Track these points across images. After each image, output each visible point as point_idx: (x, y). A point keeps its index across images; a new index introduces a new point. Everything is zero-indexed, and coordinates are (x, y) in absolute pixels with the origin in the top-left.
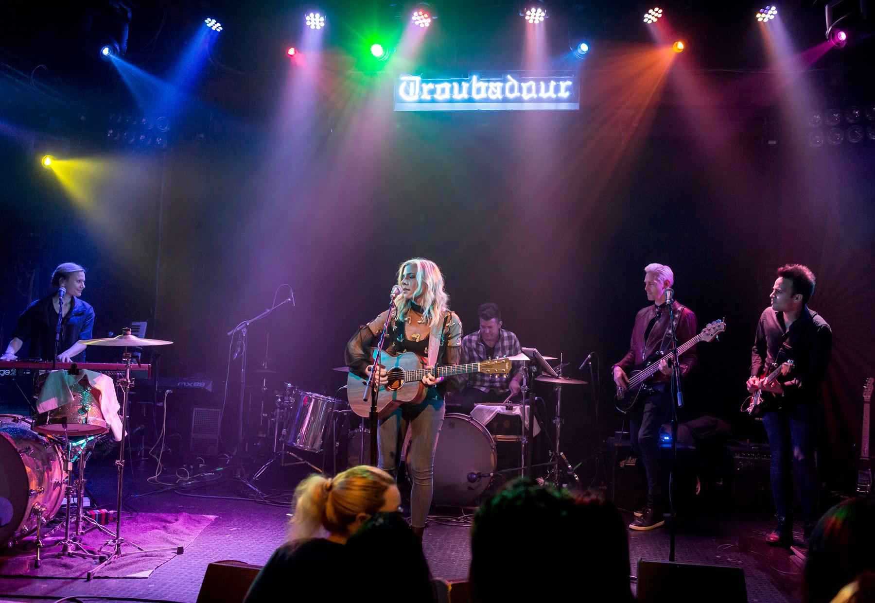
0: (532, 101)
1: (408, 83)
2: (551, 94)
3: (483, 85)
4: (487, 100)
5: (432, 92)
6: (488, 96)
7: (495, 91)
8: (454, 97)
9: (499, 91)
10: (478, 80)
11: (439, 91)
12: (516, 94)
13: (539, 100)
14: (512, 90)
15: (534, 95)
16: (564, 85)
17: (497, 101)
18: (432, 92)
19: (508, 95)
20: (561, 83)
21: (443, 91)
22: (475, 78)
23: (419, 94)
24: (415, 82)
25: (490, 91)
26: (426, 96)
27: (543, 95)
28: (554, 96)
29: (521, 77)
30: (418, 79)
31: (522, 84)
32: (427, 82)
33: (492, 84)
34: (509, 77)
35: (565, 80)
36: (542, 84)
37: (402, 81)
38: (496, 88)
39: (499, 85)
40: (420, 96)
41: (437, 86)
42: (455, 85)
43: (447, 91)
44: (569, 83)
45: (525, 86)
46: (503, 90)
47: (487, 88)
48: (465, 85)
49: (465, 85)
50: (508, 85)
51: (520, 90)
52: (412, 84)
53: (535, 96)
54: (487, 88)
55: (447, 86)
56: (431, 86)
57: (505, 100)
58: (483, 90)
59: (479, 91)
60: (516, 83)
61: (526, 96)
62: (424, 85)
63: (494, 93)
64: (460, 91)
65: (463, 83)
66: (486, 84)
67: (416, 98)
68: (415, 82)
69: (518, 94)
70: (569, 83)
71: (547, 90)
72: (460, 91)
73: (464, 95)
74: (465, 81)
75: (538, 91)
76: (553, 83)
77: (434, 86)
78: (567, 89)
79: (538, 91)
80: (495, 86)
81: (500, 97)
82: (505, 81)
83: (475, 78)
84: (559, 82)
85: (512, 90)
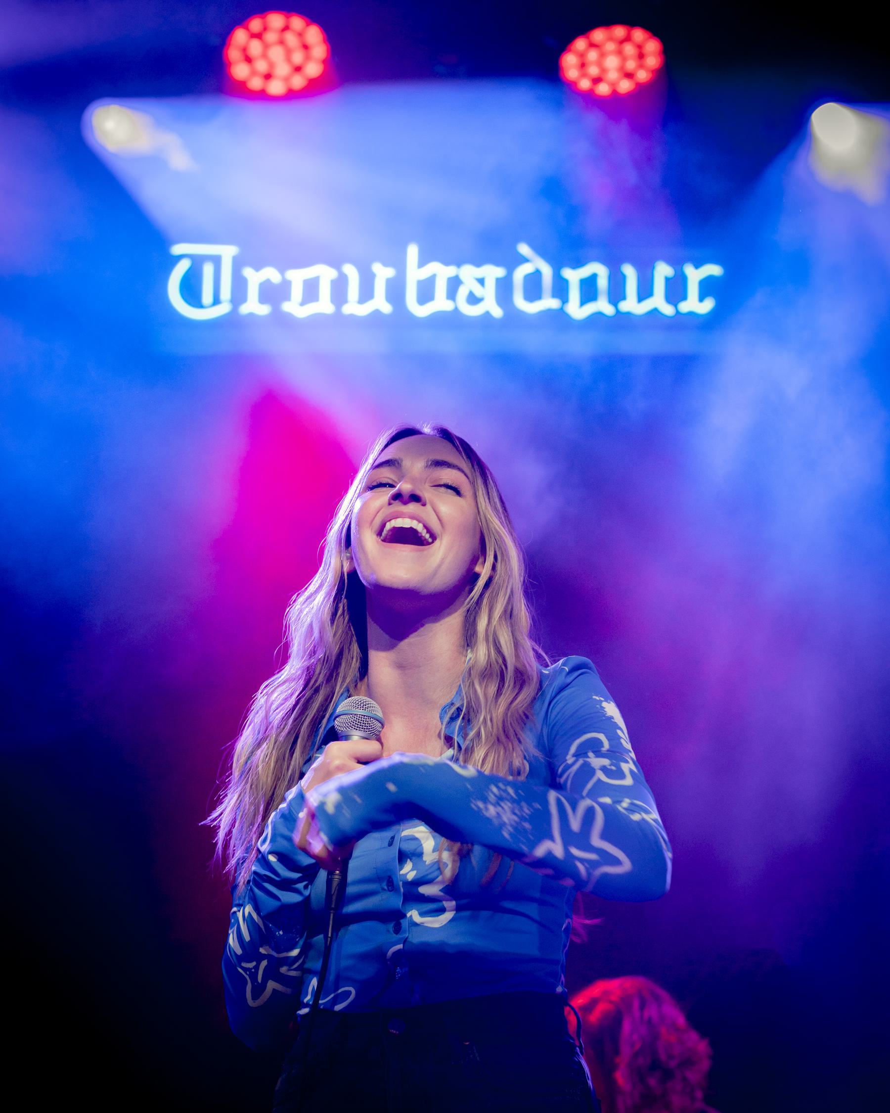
2: (658, 301)
7: (478, 291)
8: (347, 309)
9: (489, 293)
11: (297, 292)
12: (549, 303)
13: (623, 321)
14: (533, 288)
15: (603, 306)
16: (694, 275)
21: (311, 291)
22: (413, 252)
25: (462, 293)
27: (631, 305)
28: (668, 310)
30: (228, 252)
33: (468, 273)
34: (524, 249)
35: (697, 265)
38: (481, 281)
39: (493, 272)
42: (351, 271)
43: (325, 290)
44: (714, 270)
45: (573, 276)
47: (454, 284)
48: (383, 273)
51: (561, 289)
52: (208, 270)
54: (454, 284)
55: (325, 274)
56: (271, 274)
58: (441, 288)
59: (426, 292)
60: (547, 271)
61: (577, 310)
63: (473, 299)
66: (451, 271)
68: (216, 260)
70: (714, 270)
71: (645, 292)
73: (380, 303)
74: (385, 264)
75: (617, 294)
76: (663, 271)
78: (707, 287)
80: (480, 276)
81: (497, 312)
82: (513, 261)
83: (413, 252)
85: (533, 288)
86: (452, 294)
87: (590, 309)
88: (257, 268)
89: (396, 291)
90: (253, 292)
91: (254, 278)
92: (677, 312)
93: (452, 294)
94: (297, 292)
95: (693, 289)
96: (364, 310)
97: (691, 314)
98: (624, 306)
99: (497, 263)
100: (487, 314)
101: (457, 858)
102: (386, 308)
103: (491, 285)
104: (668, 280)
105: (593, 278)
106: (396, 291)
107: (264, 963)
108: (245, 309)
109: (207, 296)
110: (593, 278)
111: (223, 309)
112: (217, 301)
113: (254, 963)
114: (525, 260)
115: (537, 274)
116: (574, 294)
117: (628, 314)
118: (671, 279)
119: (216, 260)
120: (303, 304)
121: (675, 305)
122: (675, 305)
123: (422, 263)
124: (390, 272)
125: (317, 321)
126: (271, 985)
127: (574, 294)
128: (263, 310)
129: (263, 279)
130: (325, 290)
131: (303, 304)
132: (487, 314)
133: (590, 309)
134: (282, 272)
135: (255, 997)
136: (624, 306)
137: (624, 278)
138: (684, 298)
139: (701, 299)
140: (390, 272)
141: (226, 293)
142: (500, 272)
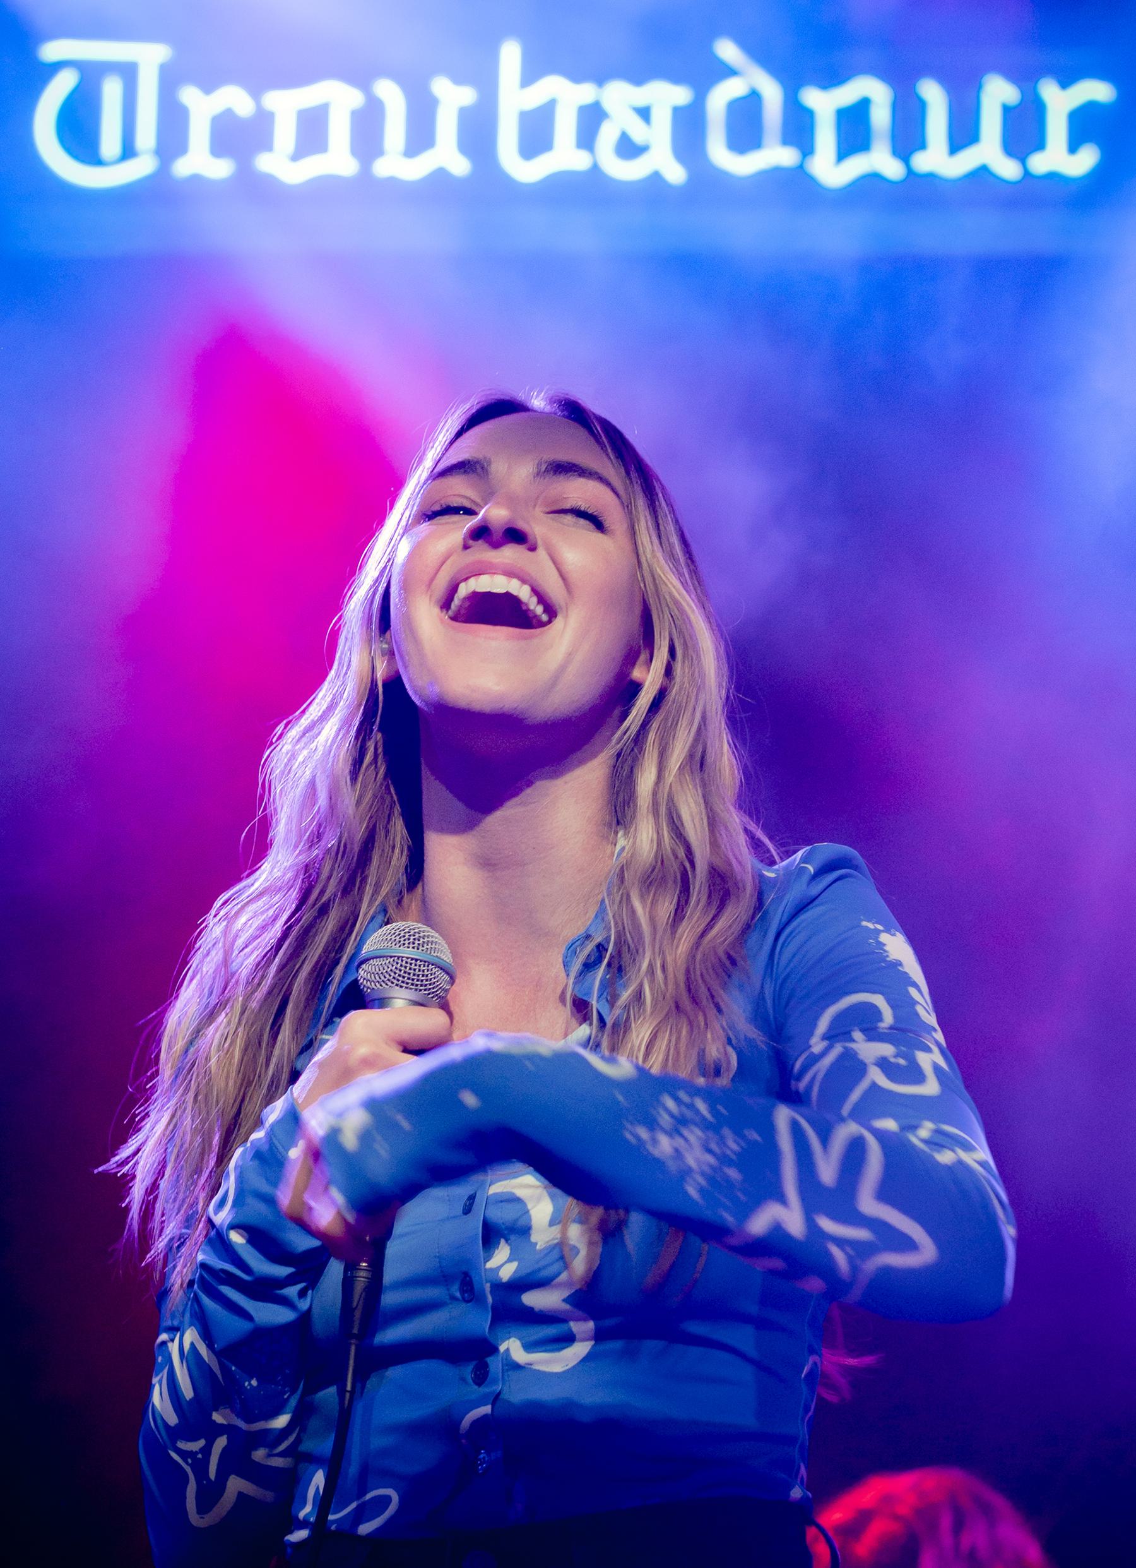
6: (595, 168)
7: (638, 132)
11: (285, 134)
22: (511, 55)
25: (607, 136)
28: (1008, 169)
34: (728, 50)
38: (644, 113)
42: (389, 92)
43: (340, 131)
52: (112, 91)
53: (892, 169)
58: (565, 127)
60: (772, 93)
62: (190, 96)
63: (628, 149)
66: (586, 93)
68: (128, 73)
74: (458, 79)
80: (641, 103)
81: (675, 174)
83: (511, 55)
86: (587, 138)
87: (857, 166)
88: (208, 86)
90: (199, 134)
92: (1027, 174)
93: (587, 138)
94: (285, 134)
95: (1057, 129)
96: (415, 169)
97: (1053, 177)
98: (923, 162)
99: (675, 78)
100: (656, 177)
101: (597, 1237)
102: (460, 166)
103: (663, 120)
104: (1007, 110)
105: (863, 105)
107: (221, 1442)
108: (183, 168)
109: (110, 142)
110: (863, 105)
111: (142, 167)
112: (128, 151)
113: (202, 1443)
114: (728, 72)
115: (753, 99)
117: (931, 177)
118: (1015, 108)
119: (128, 73)
120: (296, 157)
121: (1023, 160)
122: (1023, 160)
123: (529, 78)
124: (466, 96)
126: (235, 1485)
127: (826, 138)
128: (220, 169)
129: (218, 109)
130: (340, 131)
131: (296, 157)
132: (656, 177)
133: (857, 166)
134: (256, 93)
135: (202, 1509)
136: (923, 162)
137: (921, 106)
138: (1039, 144)
139: (1073, 147)
140: (466, 96)
141: (146, 136)
142: (681, 95)
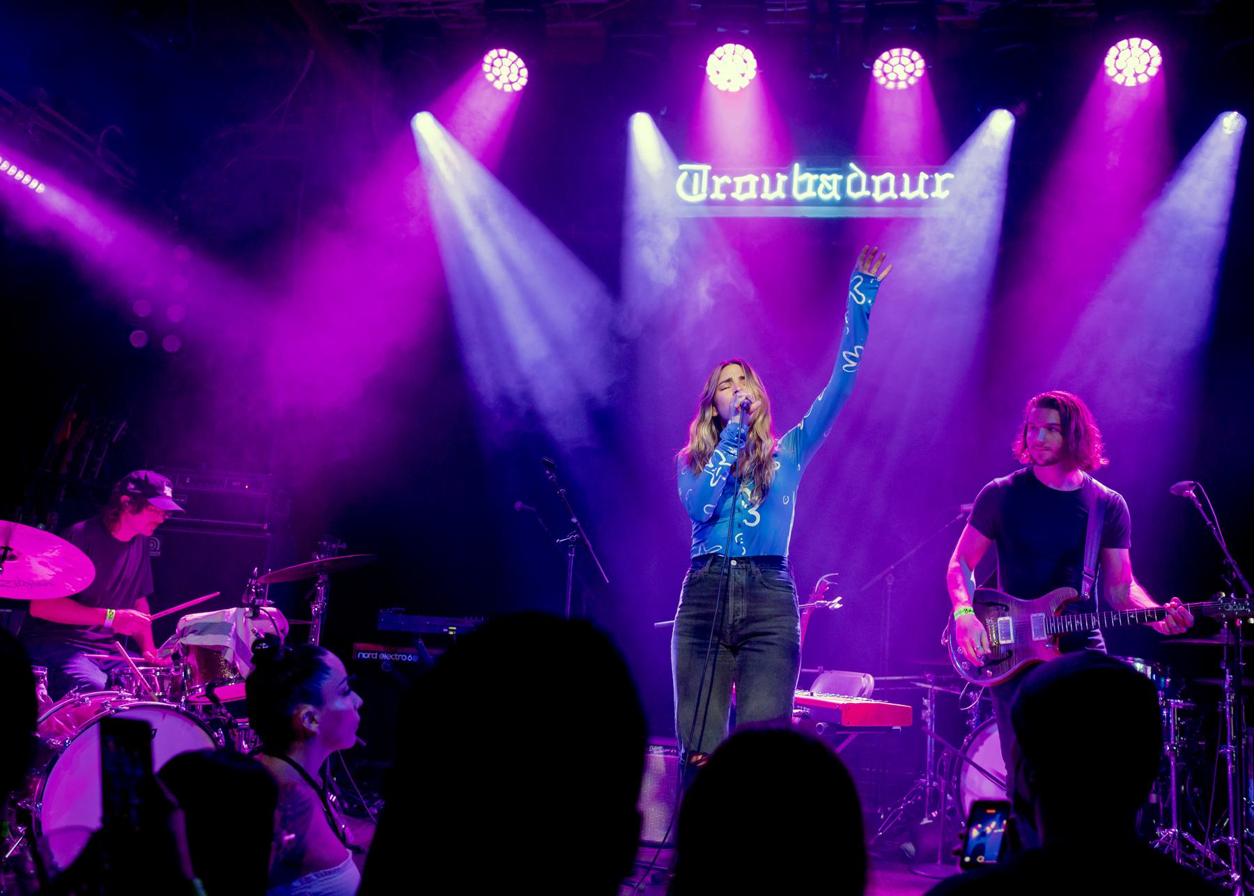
0: (888, 203)
1: (691, 174)
2: (920, 192)
3: (810, 178)
4: (816, 202)
5: (728, 189)
6: (817, 196)
7: (829, 187)
8: (763, 196)
9: (835, 188)
10: (802, 171)
11: (739, 188)
12: (864, 192)
13: (901, 203)
14: (856, 186)
15: (892, 194)
17: (832, 203)
18: (728, 189)
19: (851, 194)
20: (937, 175)
21: (746, 187)
22: (797, 167)
23: (707, 192)
24: (700, 172)
26: (718, 195)
27: (907, 194)
28: (925, 196)
29: (872, 167)
31: (874, 177)
32: (720, 175)
33: (824, 177)
34: (852, 166)
36: (906, 177)
37: (682, 171)
38: (831, 183)
39: (836, 178)
40: (708, 197)
41: (736, 179)
42: (766, 177)
43: (753, 187)
45: (877, 179)
46: (842, 187)
47: (817, 183)
48: (781, 178)
49: (781, 178)
50: (850, 178)
51: (870, 186)
52: (696, 176)
53: (895, 196)
54: (817, 183)
55: (752, 179)
56: (726, 179)
57: (845, 202)
58: (810, 186)
59: (803, 188)
60: (864, 176)
61: (879, 197)
62: (715, 178)
63: (826, 191)
64: (773, 187)
65: (778, 175)
66: (816, 177)
67: (703, 197)
68: (700, 172)
69: (868, 193)
71: (914, 187)
72: (773, 187)
73: (780, 194)
74: (783, 173)
75: (899, 188)
76: (923, 176)
77: (732, 180)
79: (899, 188)
81: (838, 198)
82: (846, 172)
84: (933, 174)
85: (856, 186)
87: (885, 196)
89: (788, 187)
91: (719, 181)
94: (739, 188)
98: (903, 194)
99: (839, 173)
100: (833, 197)
102: (783, 196)
106: (788, 187)
112: (700, 192)
116: (877, 187)
120: (742, 193)
125: (749, 203)
127: (877, 187)
131: (742, 193)
132: (833, 197)
136: (903, 194)
142: (841, 177)
